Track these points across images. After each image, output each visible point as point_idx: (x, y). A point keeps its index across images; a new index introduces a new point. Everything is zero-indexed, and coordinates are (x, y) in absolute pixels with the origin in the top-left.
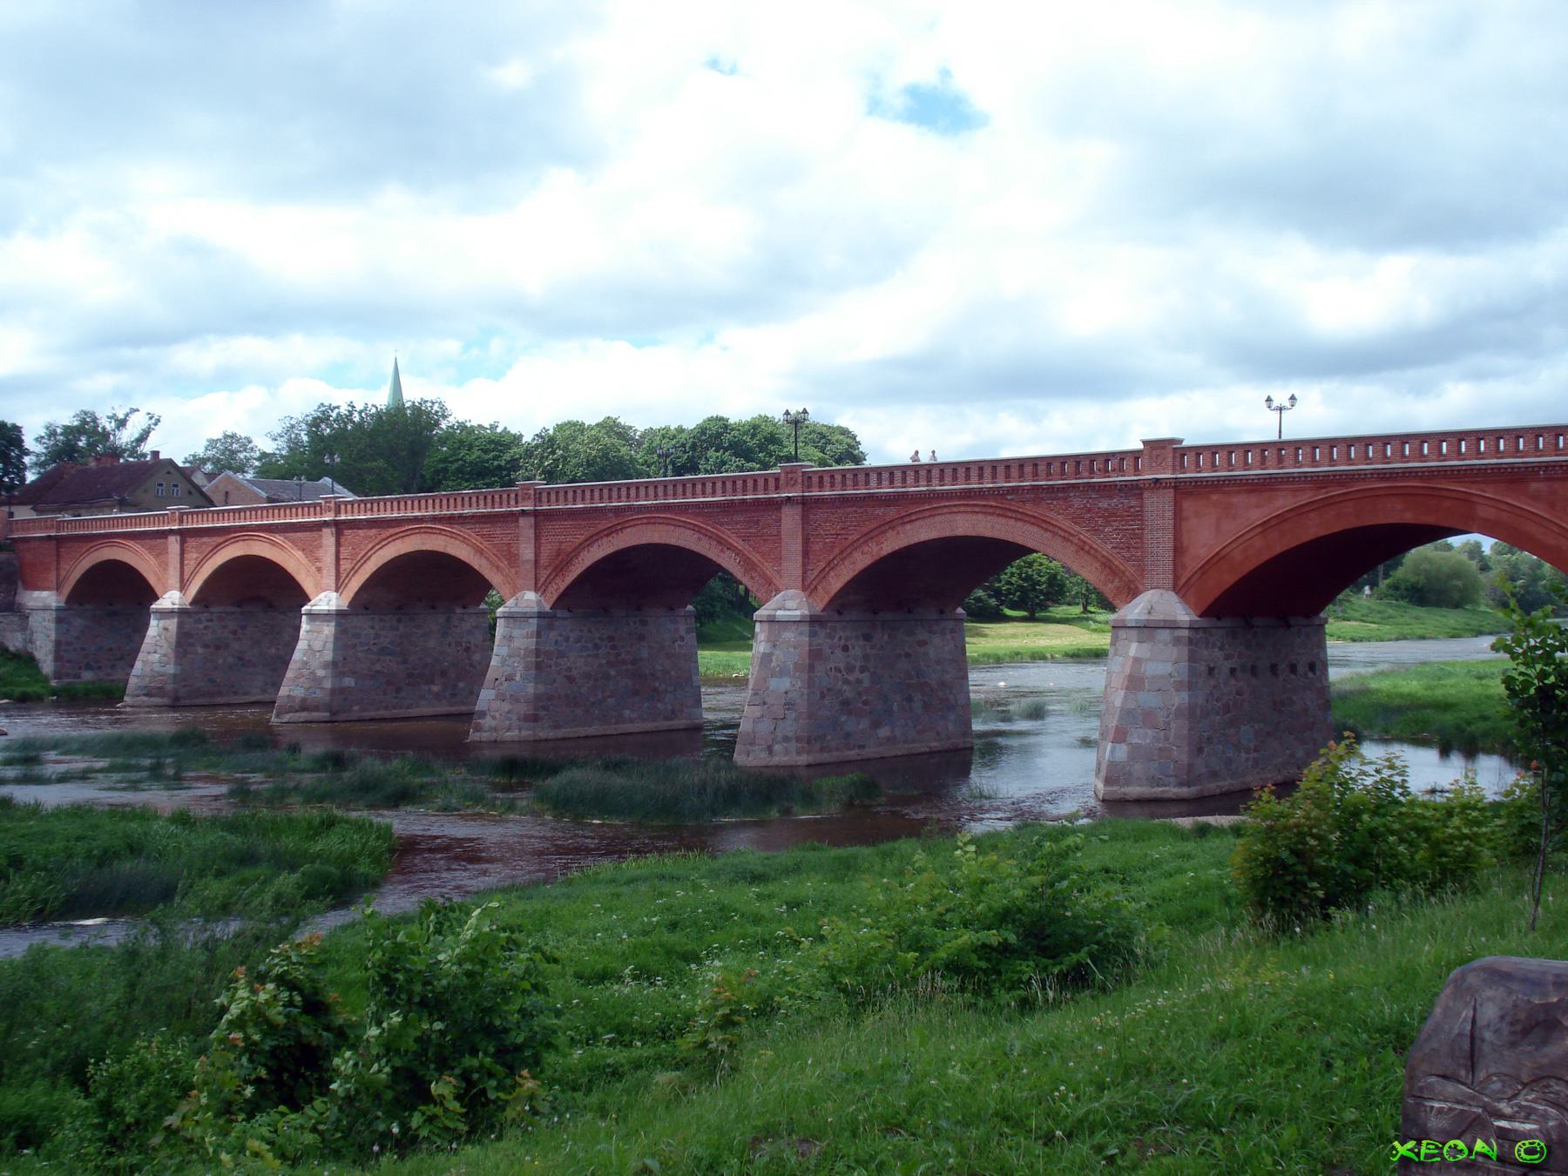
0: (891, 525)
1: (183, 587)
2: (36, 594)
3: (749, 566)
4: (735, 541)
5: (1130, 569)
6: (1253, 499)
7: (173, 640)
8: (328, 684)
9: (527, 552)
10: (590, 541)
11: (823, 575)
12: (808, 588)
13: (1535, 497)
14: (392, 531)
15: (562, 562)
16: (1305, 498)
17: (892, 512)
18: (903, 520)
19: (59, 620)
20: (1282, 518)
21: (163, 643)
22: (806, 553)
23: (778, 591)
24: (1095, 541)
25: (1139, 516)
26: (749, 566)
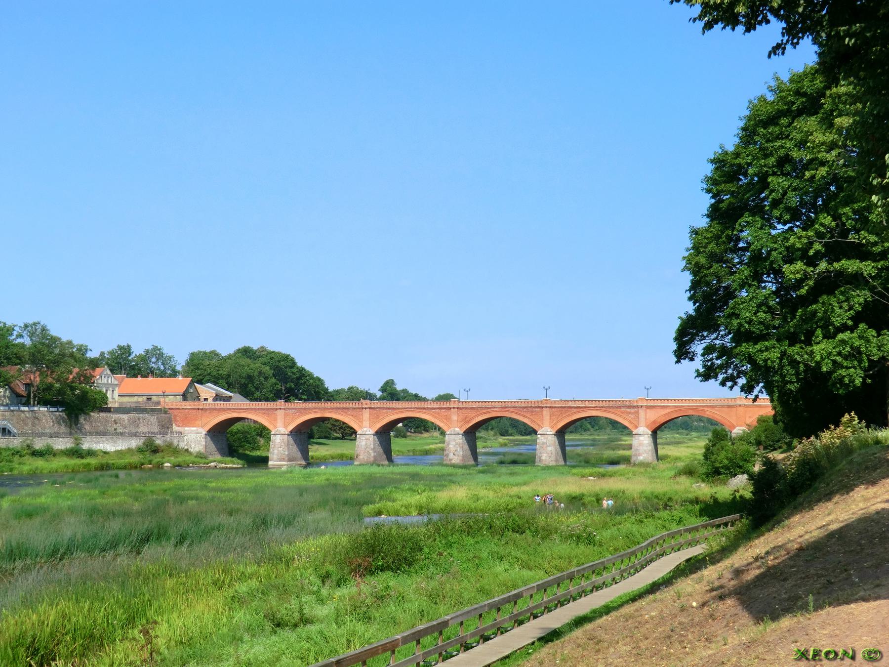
0: (575, 413)
1: (286, 427)
2: (186, 429)
3: (533, 421)
4: (528, 415)
5: (635, 423)
6: (662, 410)
7: (287, 443)
8: (372, 455)
9: (455, 418)
10: (477, 416)
11: (555, 424)
12: (552, 427)
13: (717, 411)
14: (395, 411)
15: (465, 420)
16: (673, 410)
17: (575, 410)
18: (578, 412)
19: (205, 438)
20: (668, 413)
21: (283, 444)
22: (550, 419)
23: (542, 428)
24: (627, 417)
25: (637, 412)
26: (533, 421)
